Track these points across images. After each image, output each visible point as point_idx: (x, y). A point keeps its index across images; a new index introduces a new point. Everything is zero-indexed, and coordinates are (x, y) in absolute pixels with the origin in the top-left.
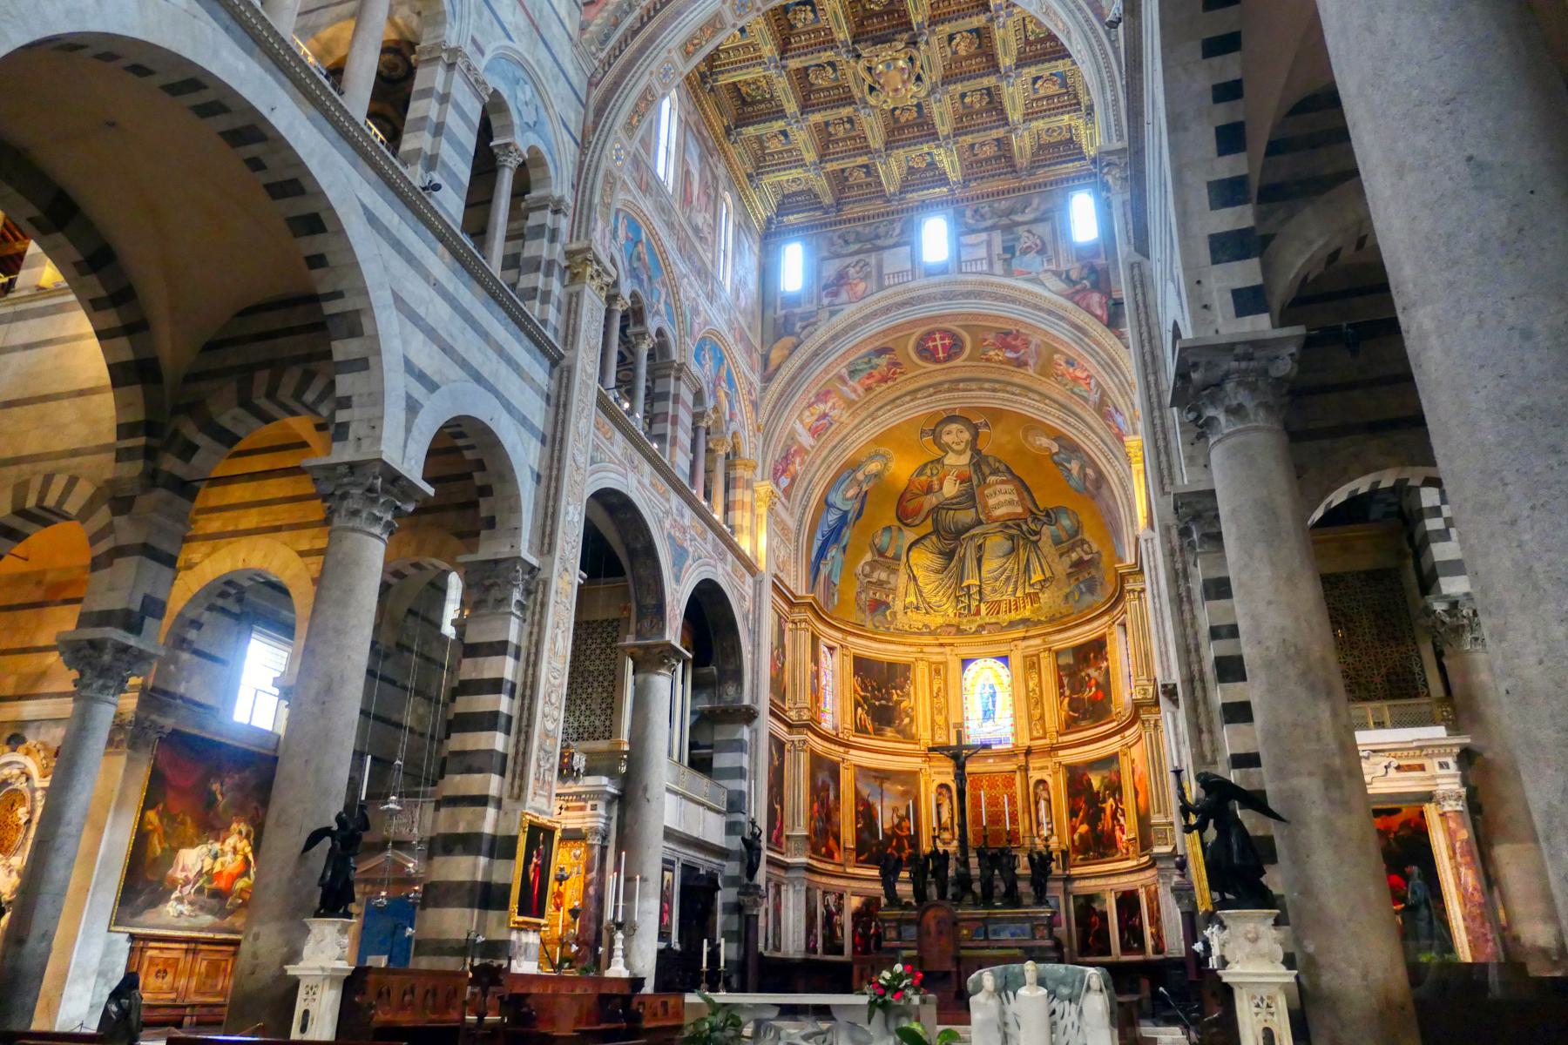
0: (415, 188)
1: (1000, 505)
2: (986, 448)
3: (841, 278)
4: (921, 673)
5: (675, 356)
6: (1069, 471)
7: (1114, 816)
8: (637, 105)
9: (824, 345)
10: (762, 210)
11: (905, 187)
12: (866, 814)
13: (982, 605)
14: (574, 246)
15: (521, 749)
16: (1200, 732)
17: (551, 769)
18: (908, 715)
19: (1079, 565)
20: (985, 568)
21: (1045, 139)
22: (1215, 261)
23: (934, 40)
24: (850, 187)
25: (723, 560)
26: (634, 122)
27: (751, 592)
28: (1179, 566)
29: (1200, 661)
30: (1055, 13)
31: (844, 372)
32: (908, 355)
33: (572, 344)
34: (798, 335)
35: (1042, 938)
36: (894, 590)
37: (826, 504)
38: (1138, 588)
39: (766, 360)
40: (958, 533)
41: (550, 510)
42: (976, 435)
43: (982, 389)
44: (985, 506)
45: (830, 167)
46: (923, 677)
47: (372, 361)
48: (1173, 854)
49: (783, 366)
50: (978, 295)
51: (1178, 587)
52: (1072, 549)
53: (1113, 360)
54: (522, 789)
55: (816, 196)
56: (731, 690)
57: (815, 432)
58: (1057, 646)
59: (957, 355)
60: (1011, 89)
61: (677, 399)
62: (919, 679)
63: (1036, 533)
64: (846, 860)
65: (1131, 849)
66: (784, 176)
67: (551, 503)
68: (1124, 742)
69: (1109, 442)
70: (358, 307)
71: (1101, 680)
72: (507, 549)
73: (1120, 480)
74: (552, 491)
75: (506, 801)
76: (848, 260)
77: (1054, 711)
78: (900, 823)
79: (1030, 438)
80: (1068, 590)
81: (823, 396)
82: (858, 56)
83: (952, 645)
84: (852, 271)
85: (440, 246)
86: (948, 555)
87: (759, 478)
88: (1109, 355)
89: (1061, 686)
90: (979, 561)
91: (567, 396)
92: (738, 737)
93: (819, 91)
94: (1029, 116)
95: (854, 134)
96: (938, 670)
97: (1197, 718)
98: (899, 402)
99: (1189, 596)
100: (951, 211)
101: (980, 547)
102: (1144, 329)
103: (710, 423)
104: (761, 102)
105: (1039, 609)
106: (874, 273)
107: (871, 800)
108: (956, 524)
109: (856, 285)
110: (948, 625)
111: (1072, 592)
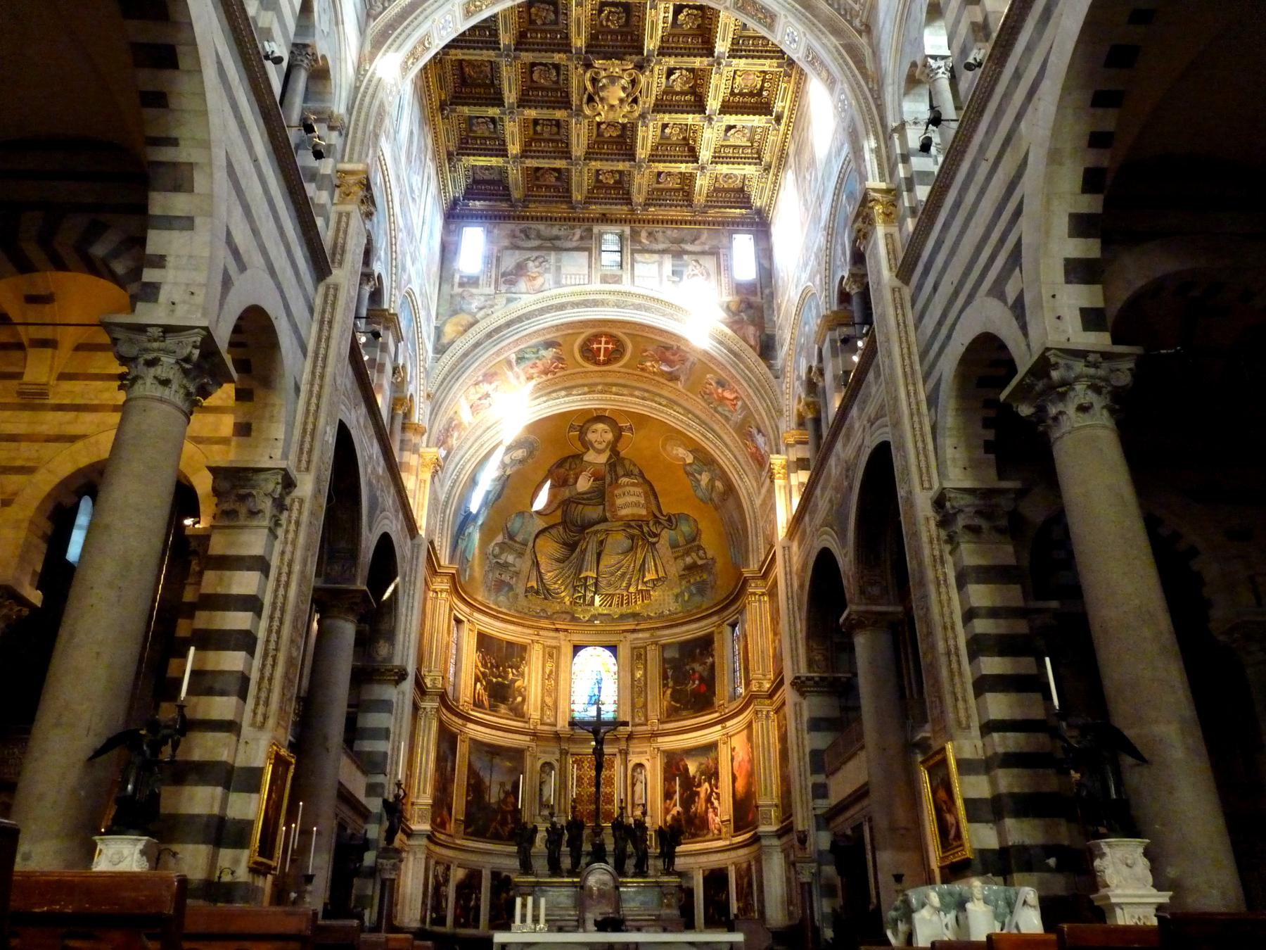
0: (259, 52)
4: (536, 657)
5: (386, 306)
6: (698, 481)
7: (708, 800)
8: (415, 47)
9: (498, 330)
10: (457, 189)
11: (589, 200)
12: (476, 787)
13: (597, 598)
14: (347, 166)
15: (267, 674)
16: (956, 700)
17: (290, 700)
18: (521, 694)
19: (691, 568)
20: (602, 564)
21: (722, 184)
22: (1068, 281)
23: (656, 69)
24: (539, 187)
25: (397, 517)
26: (409, 63)
27: (409, 555)
28: (937, 553)
29: (955, 637)
30: (822, 63)
31: (513, 357)
32: (572, 351)
33: (340, 264)
34: (474, 315)
35: (669, 906)
38: (759, 591)
39: (439, 332)
40: (585, 527)
41: (310, 427)
42: (618, 438)
43: (632, 395)
44: (613, 504)
45: (532, 163)
46: (537, 658)
47: (198, 221)
49: (458, 342)
50: (647, 309)
51: (936, 570)
52: (687, 553)
53: (763, 387)
54: (265, 717)
55: (506, 188)
56: (383, 649)
58: (663, 641)
59: (617, 360)
60: (710, 130)
61: (384, 348)
62: (534, 659)
63: (655, 535)
64: (457, 832)
65: (724, 830)
66: (482, 161)
67: (311, 419)
68: (724, 731)
69: (742, 460)
70: (192, 160)
71: (705, 674)
72: (267, 458)
73: (749, 494)
74: (313, 408)
75: (246, 729)
76: (528, 254)
77: (657, 701)
78: (506, 797)
79: (669, 448)
80: (677, 591)
82: (588, 66)
83: (566, 630)
84: (531, 264)
85: (261, 122)
86: (571, 547)
87: (424, 444)
88: (759, 381)
89: (665, 677)
90: (599, 555)
91: (332, 314)
92: (386, 697)
93: (536, 89)
94: (718, 158)
95: (557, 137)
96: (552, 653)
97: (954, 689)
98: (554, 395)
99: (945, 580)
100: (627, 230)
101: (601, 542)
102: (904, 345)
103: (399, 380)
104: (479, 86)
105: (648, 605)
106: (553, 269)
107: (481, 774)
108: (583, 520)
109: (534, 278)
110: (562, 613)
111: (682, 594)
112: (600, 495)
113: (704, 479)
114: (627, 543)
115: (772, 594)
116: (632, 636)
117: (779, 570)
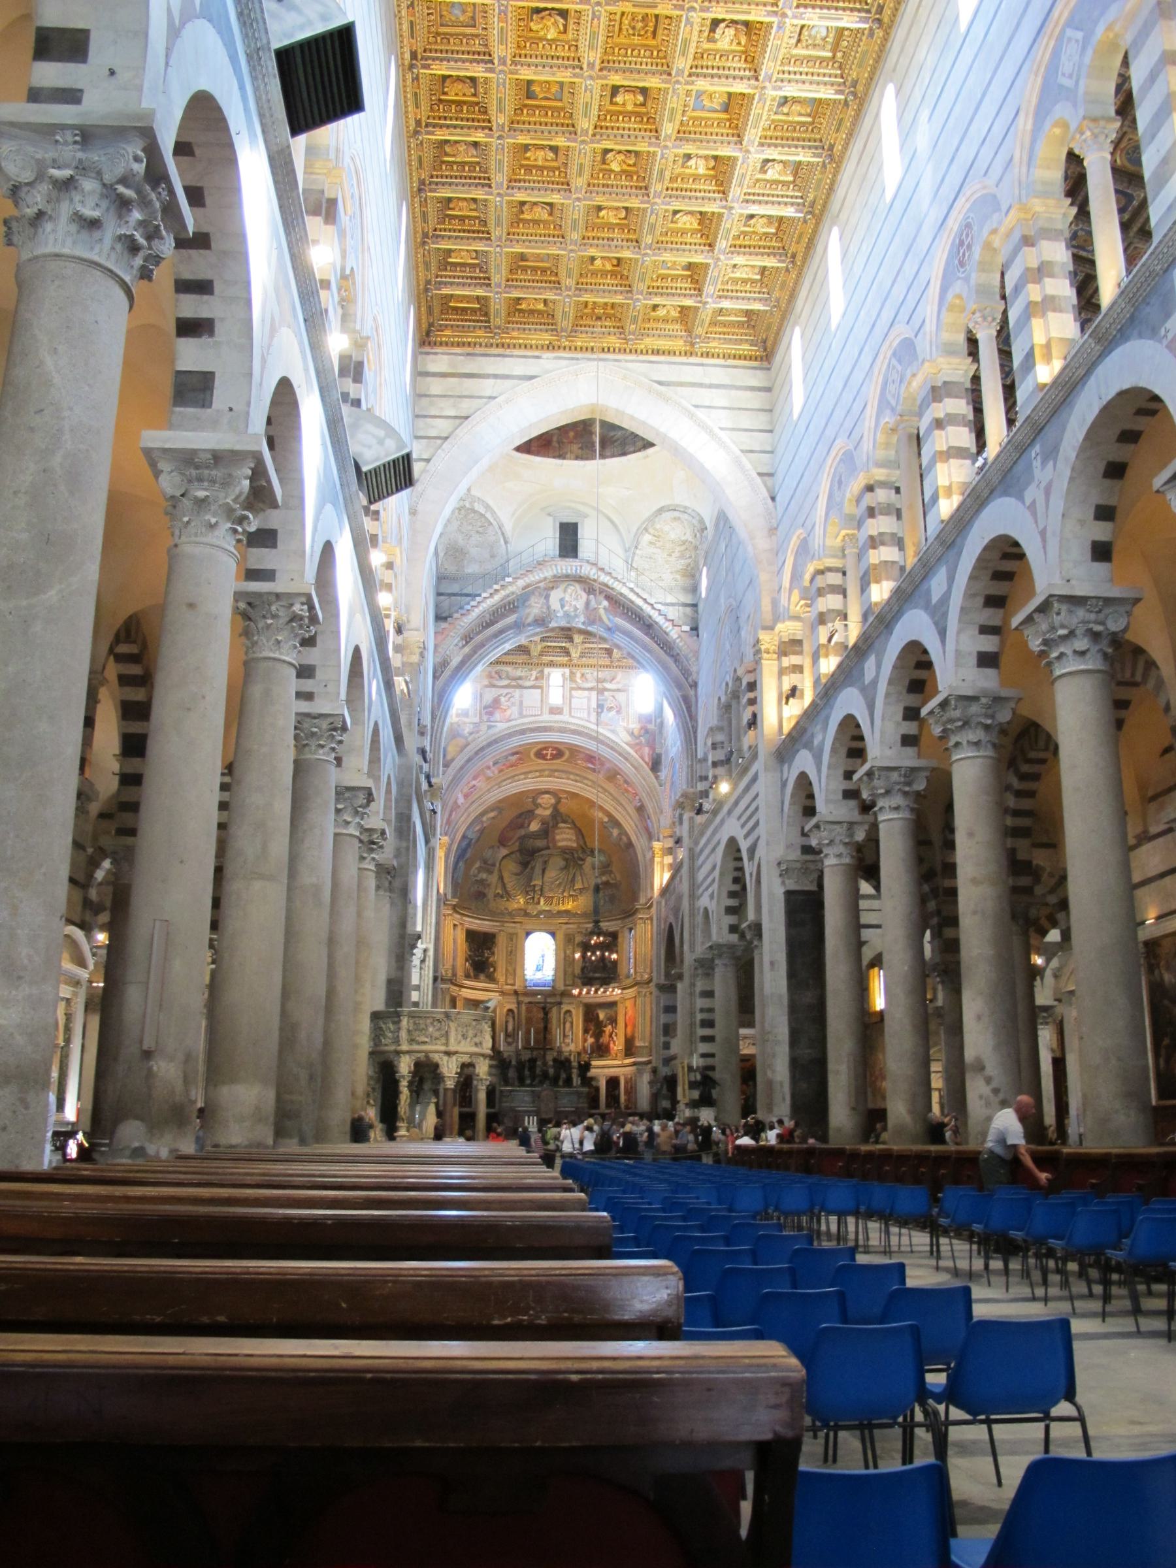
1: (563, 840)
2: (562, 809)
3: (496, 702)
7: (611, 1036)
9: (482, 749)
32: (529, 756)
34: (466, 738)
36: (489, 885)
37: (464, 837)
43: (568, 779)
44: (554, 839)
48: (649, 1062)
52: (602, 874)
57: (466, 796)
81: (475, 778)
84: (503, 699)
86: (525, 865)
90: (544, 871)
96: (512, 937)
101: (546, 862)
106: (517, 703)
112: (546, 831)
113: (615, 832)
114: (562, 863)
115: (651, 919)
116: (565, 927)
117: (653, 910)
